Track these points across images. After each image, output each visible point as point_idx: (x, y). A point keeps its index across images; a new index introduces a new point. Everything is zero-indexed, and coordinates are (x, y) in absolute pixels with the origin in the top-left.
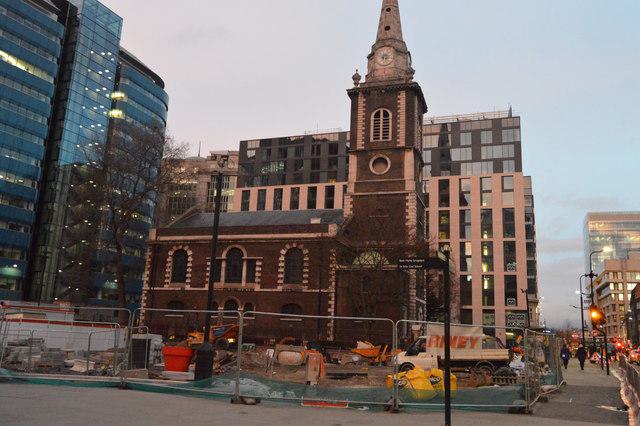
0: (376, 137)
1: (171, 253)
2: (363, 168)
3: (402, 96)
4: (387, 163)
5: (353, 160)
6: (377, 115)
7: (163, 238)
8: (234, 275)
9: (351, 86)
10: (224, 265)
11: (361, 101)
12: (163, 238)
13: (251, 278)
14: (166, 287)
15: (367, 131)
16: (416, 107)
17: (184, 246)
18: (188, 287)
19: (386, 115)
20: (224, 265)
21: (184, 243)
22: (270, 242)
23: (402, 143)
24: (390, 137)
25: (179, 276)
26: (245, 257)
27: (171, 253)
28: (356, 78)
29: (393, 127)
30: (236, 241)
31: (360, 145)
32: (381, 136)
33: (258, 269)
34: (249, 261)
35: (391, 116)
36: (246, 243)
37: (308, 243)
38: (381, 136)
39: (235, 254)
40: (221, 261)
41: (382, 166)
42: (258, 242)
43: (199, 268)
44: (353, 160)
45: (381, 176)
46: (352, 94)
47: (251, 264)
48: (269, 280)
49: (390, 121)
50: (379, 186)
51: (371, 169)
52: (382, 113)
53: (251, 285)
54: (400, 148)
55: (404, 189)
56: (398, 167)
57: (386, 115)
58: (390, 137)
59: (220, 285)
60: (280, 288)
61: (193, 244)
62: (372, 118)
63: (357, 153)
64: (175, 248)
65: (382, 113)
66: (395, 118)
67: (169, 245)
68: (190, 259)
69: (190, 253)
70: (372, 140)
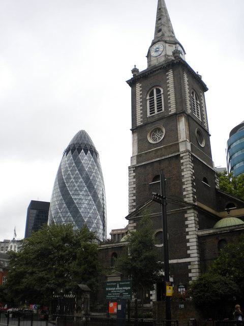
0: (152, 111)
4: (162, 132)
6: (152, 94)
9: (130, 76)
16: (186, 83)
19: (158, 91)
24: (163, 109)
28: (135, 71)
35: (162, 90)
41: (157, 135)
46: (132, 83)
49: (162, 96)
51: (151, 141)
52: (155, 91)
54: (172, 115)
55: (179, 151)
57: (158, 91)
62: (148, 98)
65: (155, 91)
66: (166, 91)
70: (149, 115)
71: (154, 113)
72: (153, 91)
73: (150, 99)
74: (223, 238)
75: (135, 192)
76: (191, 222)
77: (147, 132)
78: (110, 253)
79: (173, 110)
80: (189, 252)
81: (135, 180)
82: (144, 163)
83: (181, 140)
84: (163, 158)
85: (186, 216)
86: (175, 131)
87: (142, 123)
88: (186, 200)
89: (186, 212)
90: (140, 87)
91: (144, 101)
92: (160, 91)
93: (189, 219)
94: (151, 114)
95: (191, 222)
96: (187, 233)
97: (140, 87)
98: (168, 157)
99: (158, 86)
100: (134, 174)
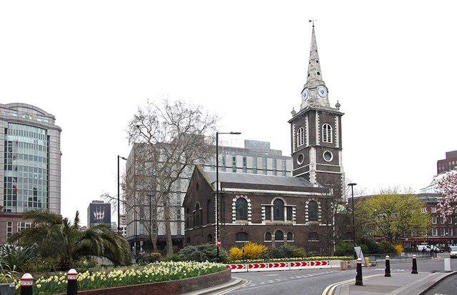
1: (235, 200)
2: (319, 158)
5: (313, 152)
7: (226, 189)
8: (279, 215)
10: (272, 209)
12: (226, 189)
13: (289, 218)
14: (234, 223)
15: (321, 135)
17: (244, 195)
18: (250, 223)
20: (272, 209)
21: (245, 194)
22: (299, 197)
23: (338, 146)
25: (242, 214)
26: (285, 205)
27: (235, 200)
30: (280, 195)
31: (318, 143)
33: (294, 212)
34: (287, 207)
36: (285, 196)
37: (320, 198)
39: (279, 205)
40: (270, 206)
42: (293, 197)
43: (257, 211)
44: (313, 152)
47: (290, 209)
48: (300, 219)
50: (329, 168)
53: (290, 222)
59: (273, 222)
60: (307, 224)
61: (250, 195)
63: (316, 147)
64: (238, 197)
66: (334, 131)
67: (233, 195)
68: (249, 205)
69: (249, 201)
79: (338, 146)
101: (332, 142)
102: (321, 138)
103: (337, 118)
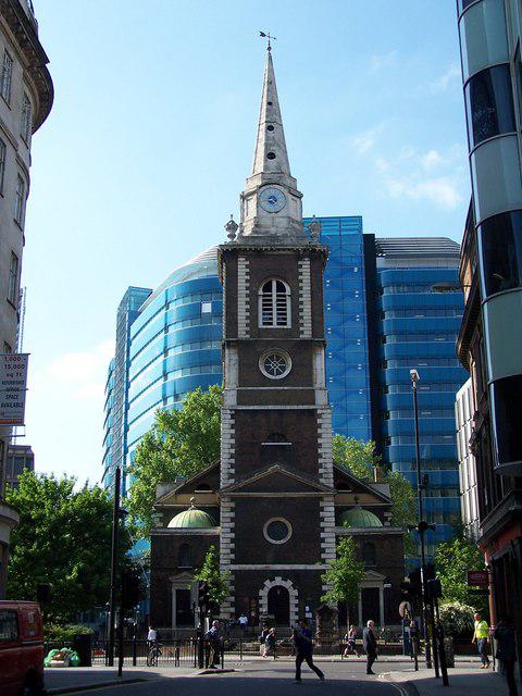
3: (306, 267)
5: (231, 360)
6: (268, 288)
11: (242, 266)
19: (281, 288)
23: (307, 334)
24: (289, 321)
28: (232, 227)
29: (292, 310)
32: (275, 321)
38: (275, 321)
41: (275, 365)
45: (276, 383)
56: (304, 373)
57: (281, 288)
58: (289, 321)
62: (261, 292)
66: (296, 296)
70: (261, 326)
71: (271, 324)
72: (270, 283)
73: (264, 296)
74: (370, 541)
75: (233, 451)
76: (329, 514)
77: (259, 355)
78: (177, 545)
79: (307, 334)
80: (323, 556)
81: (233, 431)
82: (252, 408)
83: (317, 386)
84: (288, 407)
85: (321, 504)
86: (309, 367)
87: (248, 336)
88: (322, 480)
89: (321, 499)
90: (247, 266)
91: (253, 296)
92: (284, 290)
93: (326, 509)
94: (264, 324)
95: (329, 514)
96: (323, 530)
97: (247, 266)
98: (295, 407)
99: (282, 278)
100: (233, 422)
101: (289, 326)
102: (253, 318)
103: (306, 267)
